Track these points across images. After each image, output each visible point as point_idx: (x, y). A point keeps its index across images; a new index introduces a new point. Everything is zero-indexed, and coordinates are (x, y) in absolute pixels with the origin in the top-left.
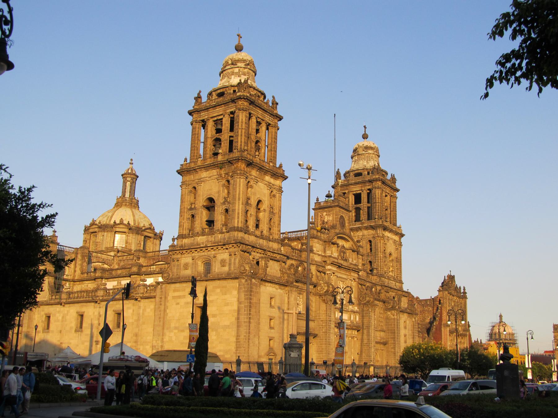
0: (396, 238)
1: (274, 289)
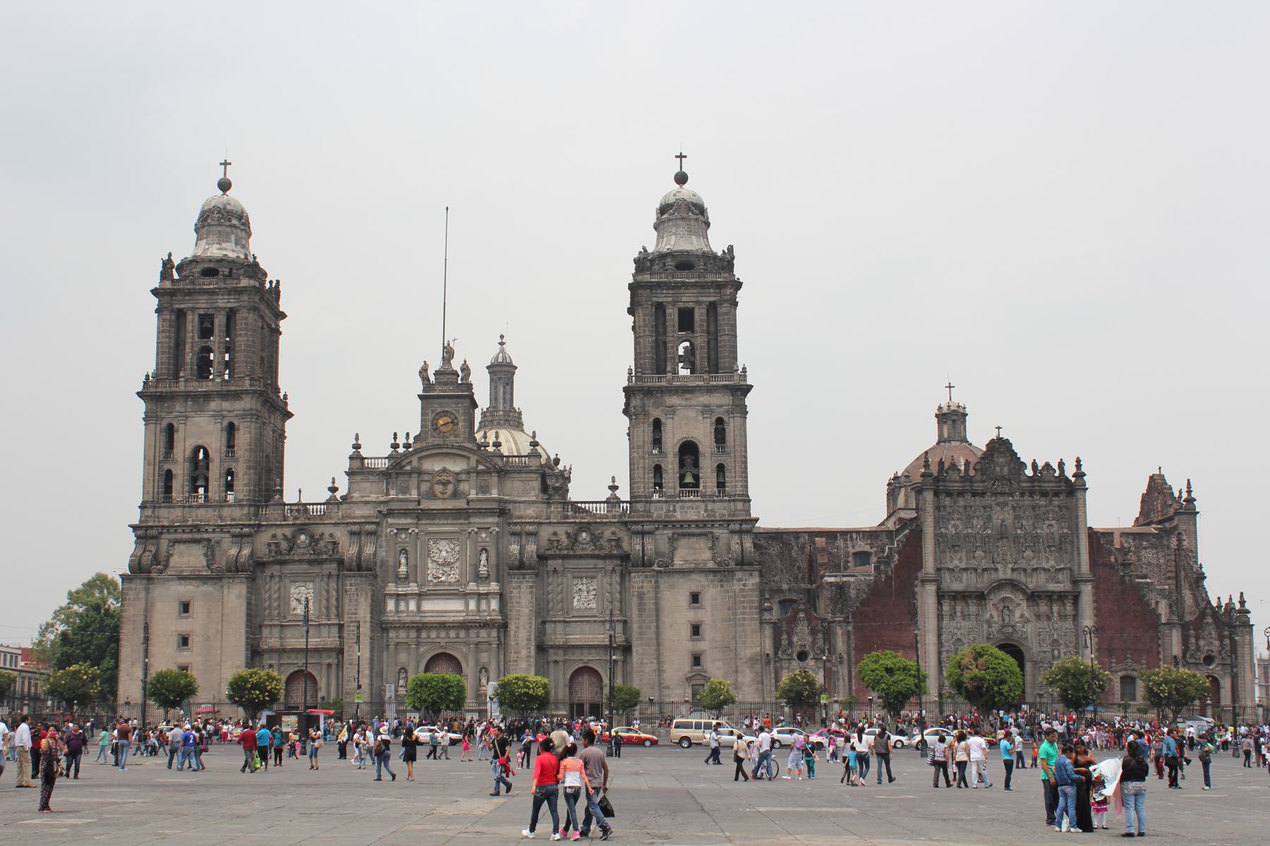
0: (721, 401)
1: (191, 587)
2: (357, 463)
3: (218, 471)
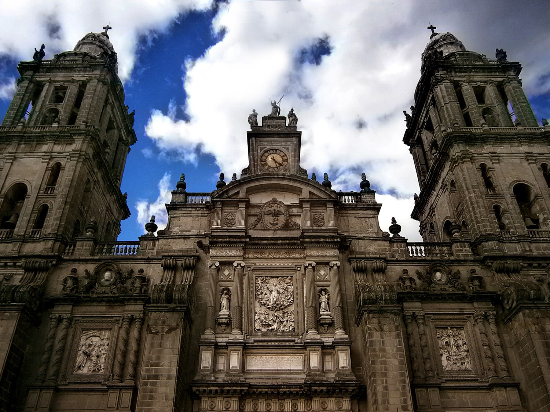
2: (180, 198)
3: (31, 207)
